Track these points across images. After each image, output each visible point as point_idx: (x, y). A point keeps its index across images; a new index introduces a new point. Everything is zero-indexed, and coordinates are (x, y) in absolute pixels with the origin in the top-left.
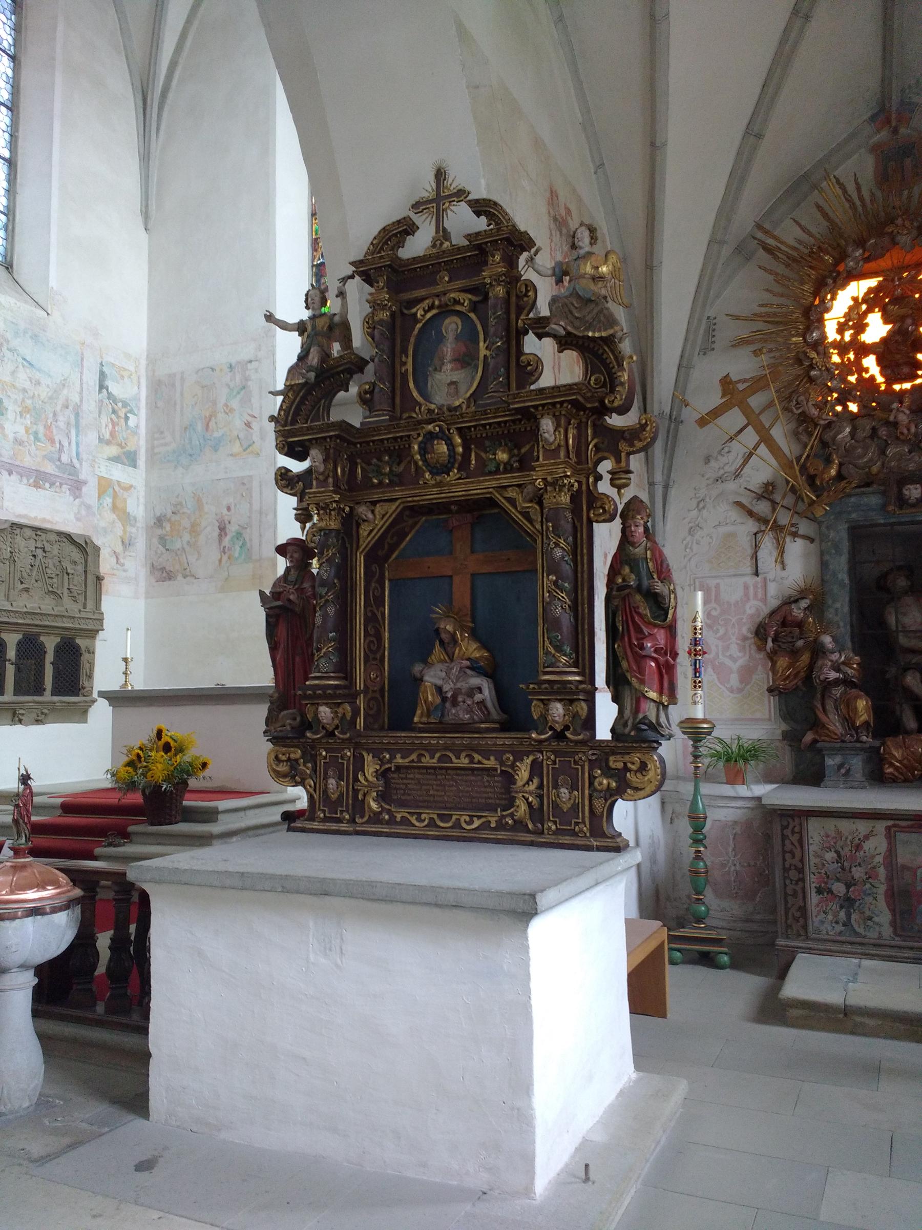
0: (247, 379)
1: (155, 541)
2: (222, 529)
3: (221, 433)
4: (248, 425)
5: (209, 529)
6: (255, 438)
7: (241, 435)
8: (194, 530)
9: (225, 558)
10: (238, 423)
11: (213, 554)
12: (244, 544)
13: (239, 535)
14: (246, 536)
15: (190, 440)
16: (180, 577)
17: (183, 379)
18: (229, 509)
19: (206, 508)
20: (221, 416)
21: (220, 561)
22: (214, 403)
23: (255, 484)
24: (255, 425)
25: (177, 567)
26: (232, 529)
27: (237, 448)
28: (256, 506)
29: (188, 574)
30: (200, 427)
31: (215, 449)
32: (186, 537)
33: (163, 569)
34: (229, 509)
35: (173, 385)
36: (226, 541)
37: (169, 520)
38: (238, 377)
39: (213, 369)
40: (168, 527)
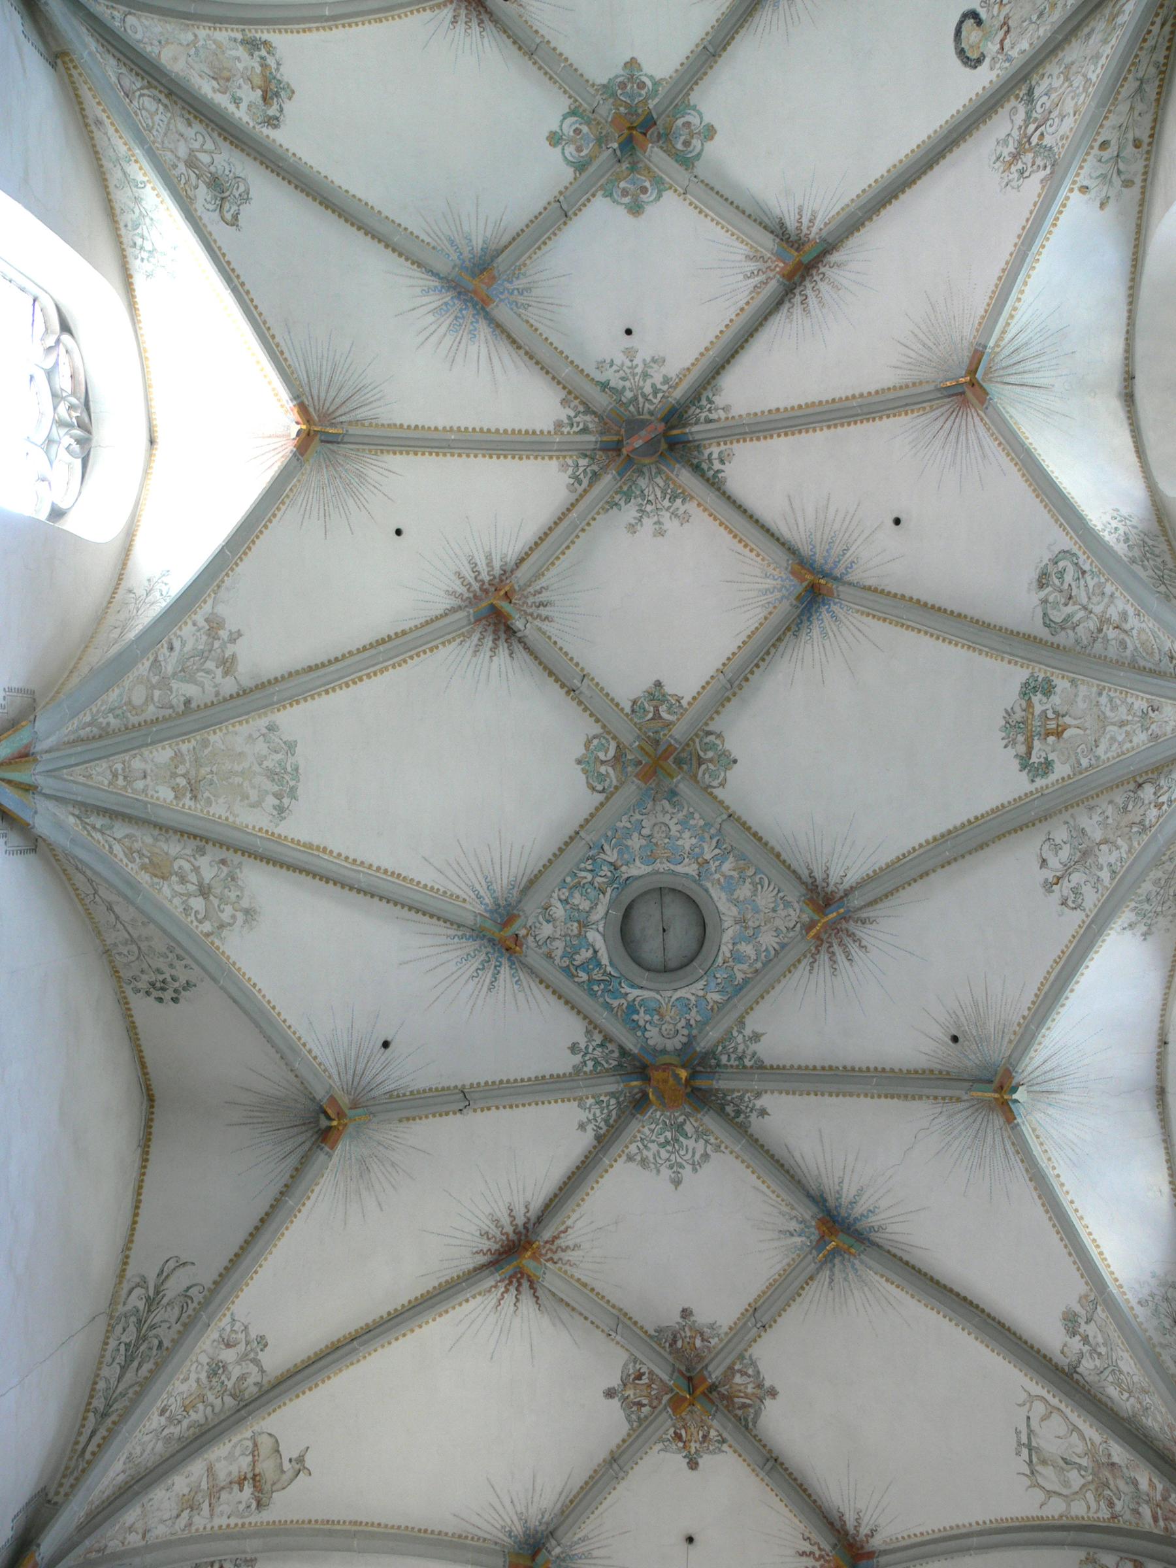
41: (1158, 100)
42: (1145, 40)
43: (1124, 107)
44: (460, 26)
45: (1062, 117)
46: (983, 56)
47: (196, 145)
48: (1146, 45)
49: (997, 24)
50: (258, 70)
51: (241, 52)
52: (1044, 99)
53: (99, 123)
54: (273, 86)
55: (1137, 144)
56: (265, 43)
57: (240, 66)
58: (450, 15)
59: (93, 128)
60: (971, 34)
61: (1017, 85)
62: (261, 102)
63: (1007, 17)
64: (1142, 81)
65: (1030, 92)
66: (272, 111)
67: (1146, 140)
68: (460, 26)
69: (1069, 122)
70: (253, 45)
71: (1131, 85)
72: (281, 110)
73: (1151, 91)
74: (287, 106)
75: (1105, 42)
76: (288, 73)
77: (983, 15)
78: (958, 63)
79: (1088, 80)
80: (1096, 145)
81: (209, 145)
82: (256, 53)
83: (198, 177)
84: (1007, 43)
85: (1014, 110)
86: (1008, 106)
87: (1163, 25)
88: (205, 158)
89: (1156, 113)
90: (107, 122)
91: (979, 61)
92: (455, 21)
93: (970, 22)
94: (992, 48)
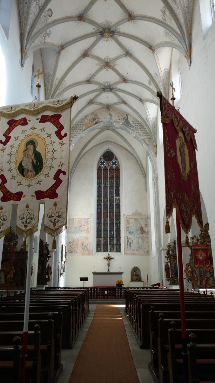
0: (88, 221)
1: (69, 246)
2: (82, 245)
3: (83, 229)
4: (88, 228)
5: (80, 245)
6: (89, 231)
7: (87, 230)
8: (77, 244)
9: (83, 250)
10: (86, 228)
11: (81, 249)
12: (87, 248)
13: (86, 246)
14: (87, 246)
15: (77, 229)
16: (74, 252)
17: (75, 219)
18: (84, 242)
19: (79, 241)
20: (83, 226)
21: (82, 250)
22: (81, 224)
23: (89, 238)
24: (89, 229)
25: (73, 251)
26: (84, 245)
27: (85, 232)
28: (89, 241)
29: (75, 252)
30: (78, 228)
31: (82, 232)
32: (75, 246)
33: (70, 251)
34: (84, 242)
35: (73, 220)
36: (83, 247)
37: (72, 243)
38: (86, 220)
39: (81, 219)
40: (72, 244)
41: (19, 11)
42: (25, 23)
43: (25, 11)
44: (133, 11)
45: (34, 7)
46: (48, 11)
47: (176, 10)
48: (24, 23)
49: (46, 16)
50: (165, 16)
51: (167, 20)
52: (37, 8)
53: (189, 21)
54: (163, 13)
55: (20, 2)
56: (163, 19)
57: (167, 18)
58: (135, 13)
59: (191, 20)
60: (50, 14)
61: (42, 9)
62: (166, 11)
63: (45, 18)
64: (23, 16)
65: (39, 8)
66: (164, 9)
67: (19, 3)
68: (133, 11)
69: (33, 7)
70: (165, 20)
71: (25, 15)
72: (163, 8)
73: (21, 14)
74: (162, 8)
75: (30, 21)
76: (161, 13)
77: (49, 17)
78: (52, 9)
79: (32, 15)
80: (27, 3)
81: (175, 9)
82: (165, 18)
83: (177, 5)
84: (44, 15)
85: (41, 4)
86: (42, 4)
87: (23, 26)
88: (176, 7)
89: (19, 9)
90: (188, 21)
91: (48, 10)
92: (134, 12)
93: (50, 15)
94: (46, 13)
